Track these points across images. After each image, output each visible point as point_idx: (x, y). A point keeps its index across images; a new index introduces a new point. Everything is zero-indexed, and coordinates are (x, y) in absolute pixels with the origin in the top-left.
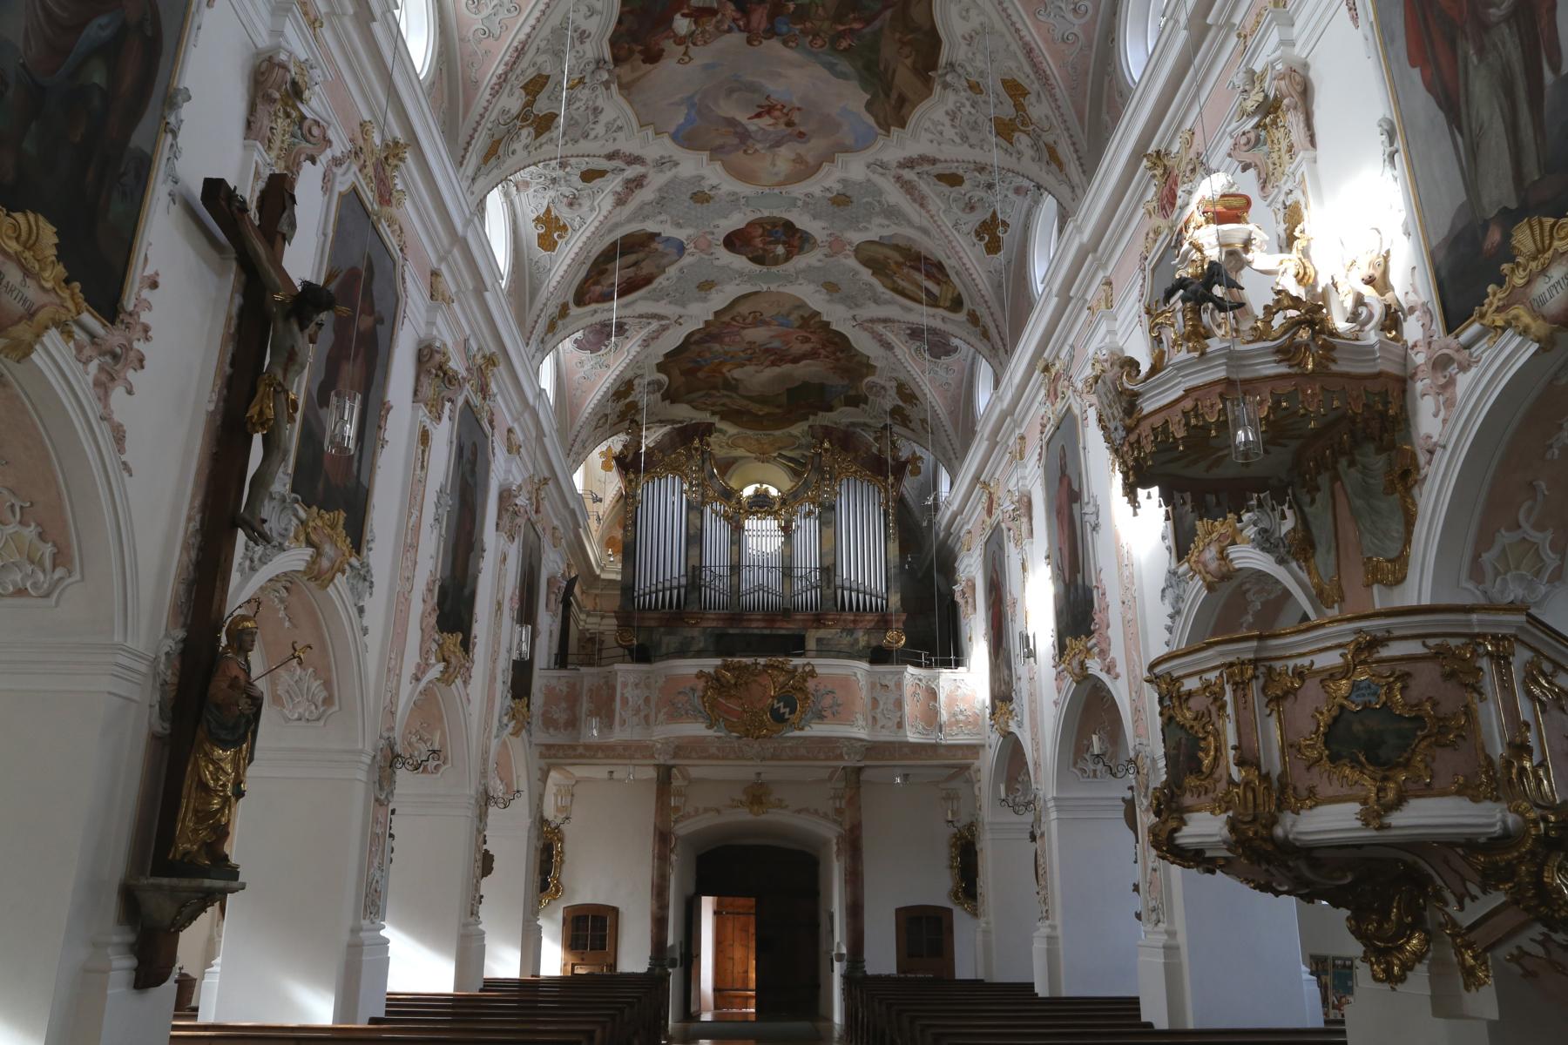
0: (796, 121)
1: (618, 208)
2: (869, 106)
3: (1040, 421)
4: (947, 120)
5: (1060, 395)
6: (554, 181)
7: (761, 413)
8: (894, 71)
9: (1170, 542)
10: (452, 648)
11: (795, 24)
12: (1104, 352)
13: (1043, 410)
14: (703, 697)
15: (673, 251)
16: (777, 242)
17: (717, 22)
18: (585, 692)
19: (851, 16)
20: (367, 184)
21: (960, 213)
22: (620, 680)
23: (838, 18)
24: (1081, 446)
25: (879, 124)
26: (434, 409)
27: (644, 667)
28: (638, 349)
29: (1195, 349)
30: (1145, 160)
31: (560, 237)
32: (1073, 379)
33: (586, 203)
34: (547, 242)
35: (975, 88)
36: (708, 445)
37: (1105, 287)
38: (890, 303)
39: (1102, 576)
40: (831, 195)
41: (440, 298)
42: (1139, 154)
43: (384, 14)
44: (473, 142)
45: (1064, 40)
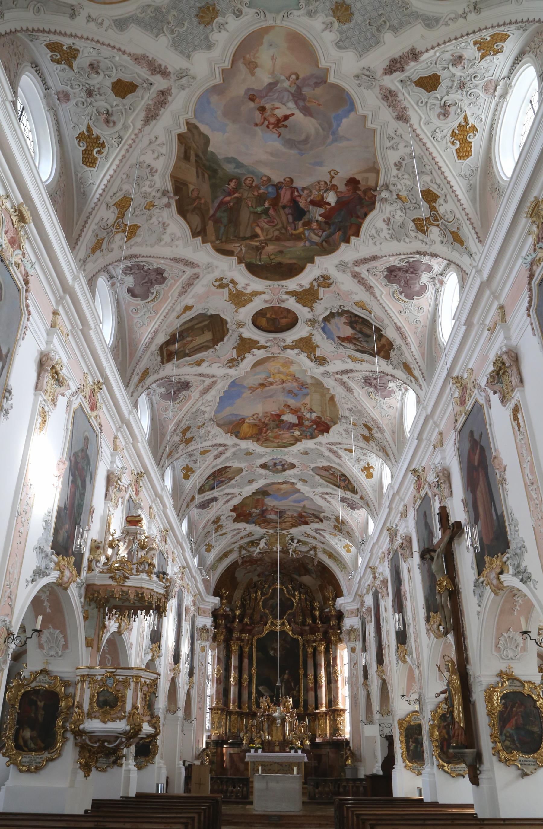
0: (257, 112)
2: (207, 141)
8: (198, 177)
11: (263, 193)
17: (310, 196)
23: (239, 200)
25: (196, 127)
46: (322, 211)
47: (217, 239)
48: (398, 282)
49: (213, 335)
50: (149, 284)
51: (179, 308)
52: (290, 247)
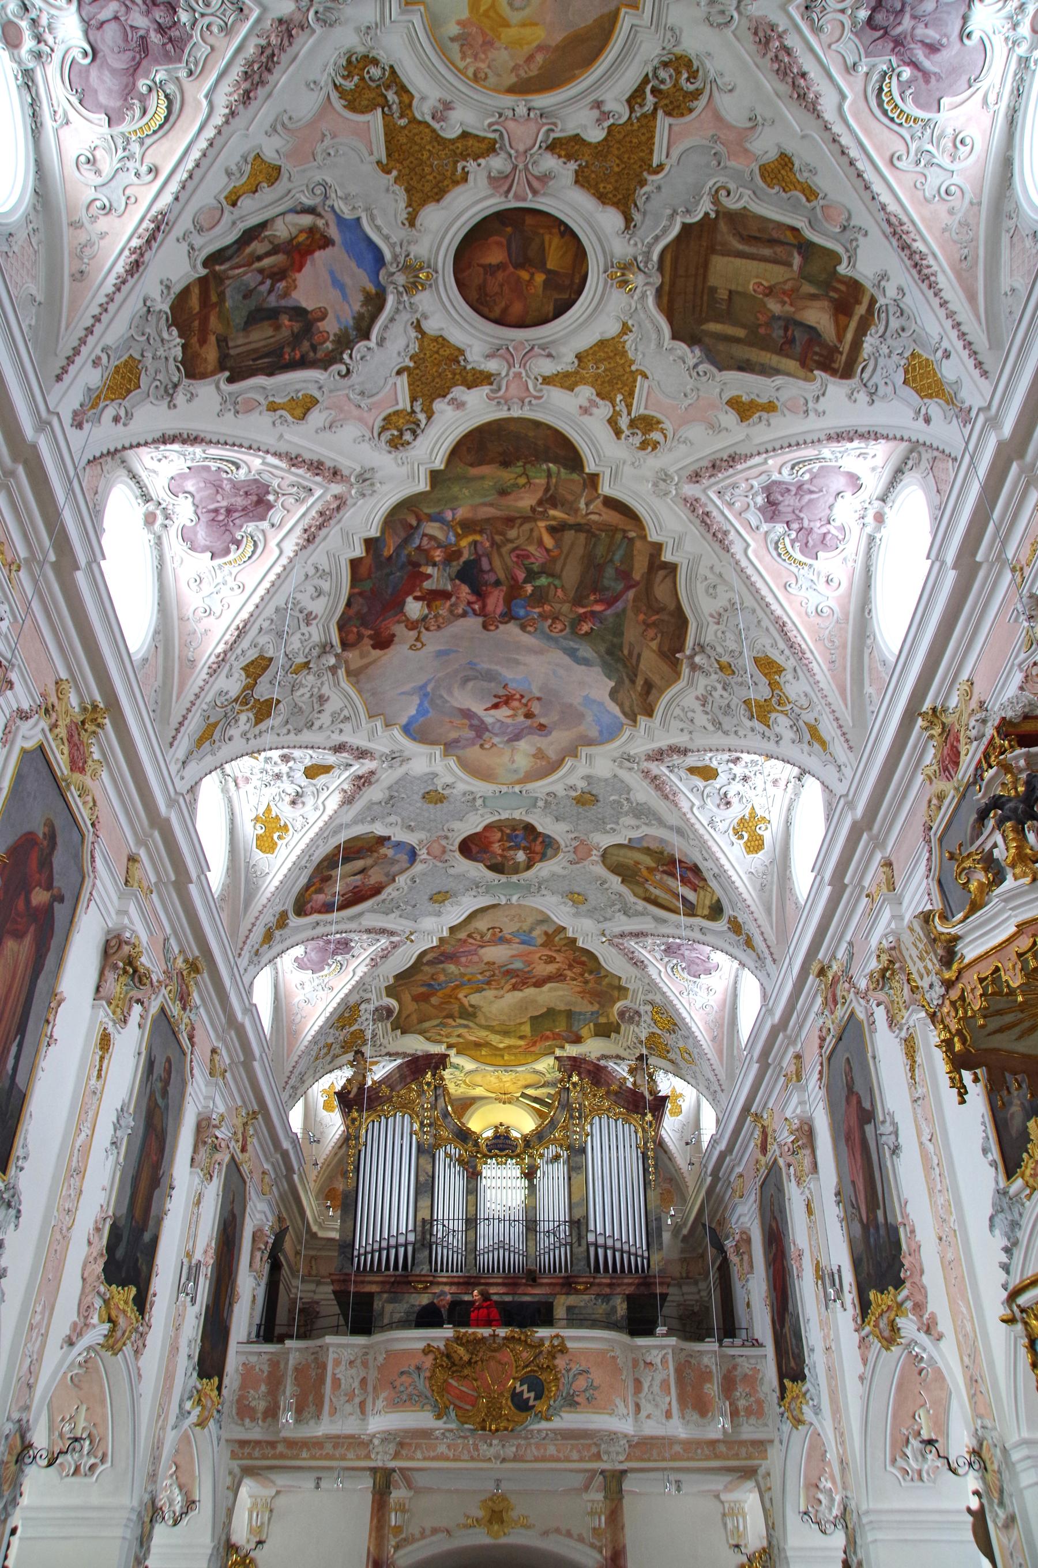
0: (536, 712)
1: (345, 807)
2: (613, 694)
3: (817, 1033)
4: (697, 705)
5: (840, 1001)
6: (278, 776)
7: (501, 1046)
8: (639, 655)
9: (995, 1154)
10: (122, 1305)
12: (891, 939)
13: (821, 1021)
14: (430, 1378)
15: (404, 857)
16: (518, 847)
18: (290, 1372)
19: (592, 598)
20: (58, 747)
21: (715, 809)
22: (331, 1356)
23: (578, 600)
24: (870, 1055)
26: (119, 1010)
27: (361, 1340)
28: (365, 969)
29: (1024, 875)
30: (920, 719)
31: (279, 837)
32: (855, 979)
33: (310, 801)
34: (267, 844)
35: (725, 668)
36: (442, 1079)
37: (885, 869)
38: (642, 914)
39: (909, 1209)
40: (574, 794)
41: (136, 885)
42: (911, 714)
43: (89, 564)
44: (186, 723)
45: (818, 613)
46: (427, 585)
47: (631, 540)
48: (235, 485)
49: (706, 265)
50: (806, 487)
51: (760, 432)
52: (485, 504)
